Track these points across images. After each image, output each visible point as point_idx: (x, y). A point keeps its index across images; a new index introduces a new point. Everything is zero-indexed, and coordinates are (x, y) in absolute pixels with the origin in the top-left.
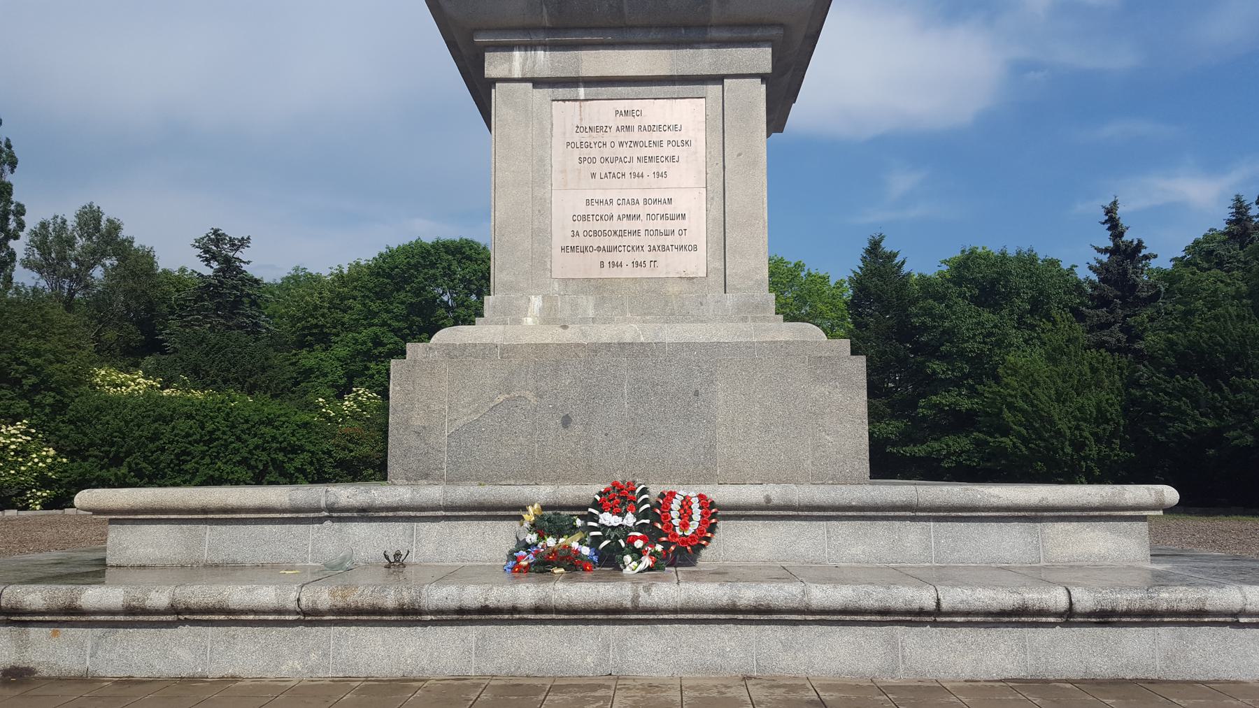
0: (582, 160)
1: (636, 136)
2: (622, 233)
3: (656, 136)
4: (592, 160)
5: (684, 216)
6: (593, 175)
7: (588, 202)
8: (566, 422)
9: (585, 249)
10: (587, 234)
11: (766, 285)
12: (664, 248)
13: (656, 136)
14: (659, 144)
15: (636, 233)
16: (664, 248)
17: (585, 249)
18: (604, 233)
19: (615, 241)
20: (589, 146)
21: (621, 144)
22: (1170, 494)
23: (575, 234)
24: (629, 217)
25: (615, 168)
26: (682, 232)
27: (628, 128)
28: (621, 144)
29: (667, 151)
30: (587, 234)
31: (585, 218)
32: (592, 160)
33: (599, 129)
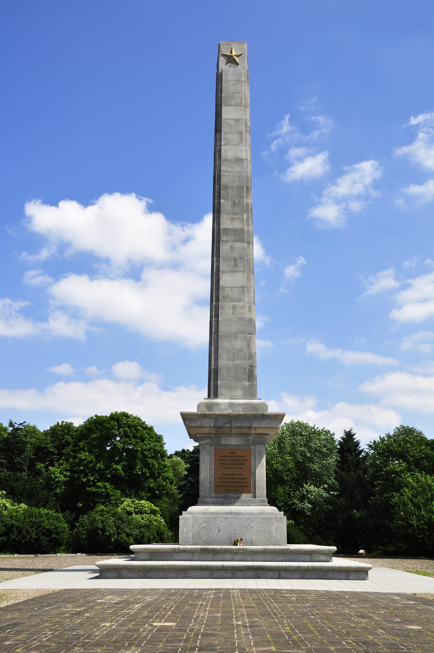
0: (221, 464)
1: (235, 458)
2: (231, 483)
3: (239, 458)
4: (224, 464)
5: (246, 479)
6: (224, 468)
7: (223, 475)
8: (219, 531)
9: (222, 486)
10: (223, 482)
11: (265, 496)
12: (241, 486)
13: (239, 458)
14: (239, 460)
15: (234, 482)
16: (241, 486)
17: (222, 486)
18: (227, 482)
19: (229, 484)
20: (223, 460)
21: (231, 460)
22: (335, 548)
23: (220, 482)
24: (233, 478)
25: (230, 466)
26: (246, 482)
27: (233, 457)
28: (231, 460)
29: (242, 462)
30: (223, 482)
31: (222, 478)
32: (224, 464)
33: (225, 456)
